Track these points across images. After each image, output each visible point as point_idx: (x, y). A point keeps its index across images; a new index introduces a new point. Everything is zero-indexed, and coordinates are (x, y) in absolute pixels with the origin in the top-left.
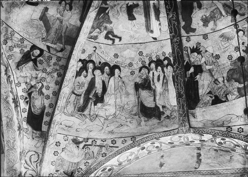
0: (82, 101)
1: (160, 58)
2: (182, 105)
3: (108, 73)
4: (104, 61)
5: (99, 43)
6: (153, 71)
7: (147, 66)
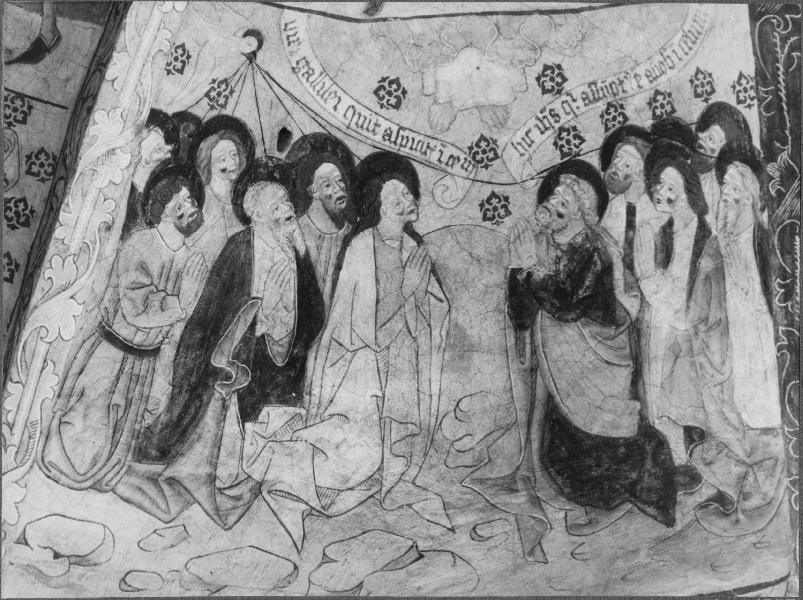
0: (161, 388)
1: (674, 111)
3: (332, 205)
4: (311, 128)
7: (594, 160)
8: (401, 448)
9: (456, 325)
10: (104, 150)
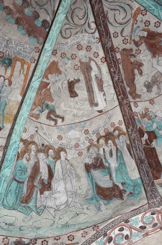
1: (108, 131)
2: (146, 172)
6: (103, 147)
7: (96, 143)
8: (71, 196)
9: (77, 174)
10: (14, 141)
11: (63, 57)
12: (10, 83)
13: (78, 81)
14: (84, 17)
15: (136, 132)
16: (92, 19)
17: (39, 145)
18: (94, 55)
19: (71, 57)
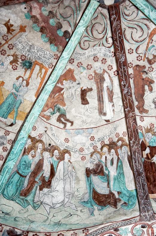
1: (113, 140)
2: (142, 185)
5: (51, 124)
7: (100, 150)
8: (68, 197)
9: (77, 176)
11: (79, 66)
12: (28, 84)
13: (91, 90)
14: (103, 32)
15: (137, 144)
16: (109, 34)
17: (46, 144)
18: (108, 67)
19: (87, 67)
